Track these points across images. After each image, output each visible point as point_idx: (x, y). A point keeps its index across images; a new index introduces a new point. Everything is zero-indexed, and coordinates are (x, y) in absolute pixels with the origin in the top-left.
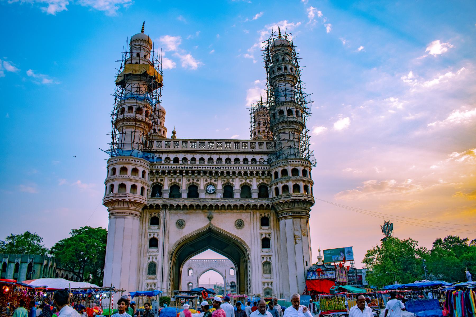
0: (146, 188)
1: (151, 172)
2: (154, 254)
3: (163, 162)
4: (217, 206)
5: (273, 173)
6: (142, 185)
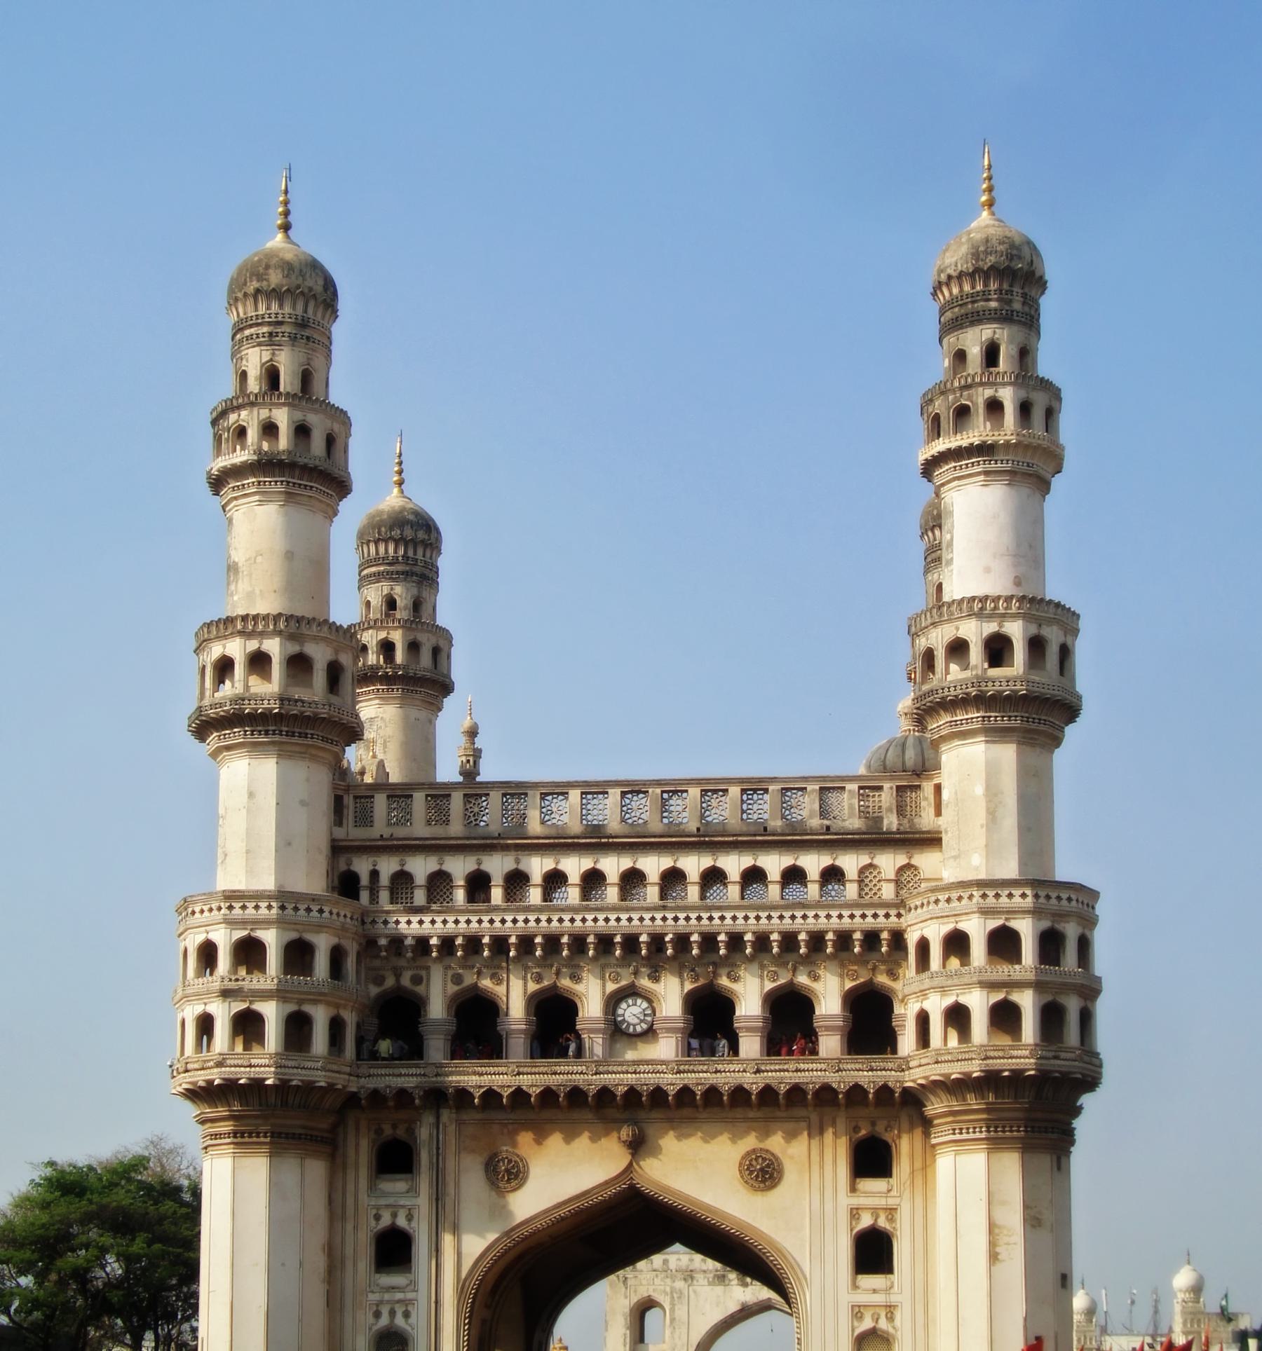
0: (350, 1018)
1: (369, 945)
2: (399, 1296)
3: (420, 897)
4: (658, 1094)
5: (912, 939)
6: (332, 1012)
